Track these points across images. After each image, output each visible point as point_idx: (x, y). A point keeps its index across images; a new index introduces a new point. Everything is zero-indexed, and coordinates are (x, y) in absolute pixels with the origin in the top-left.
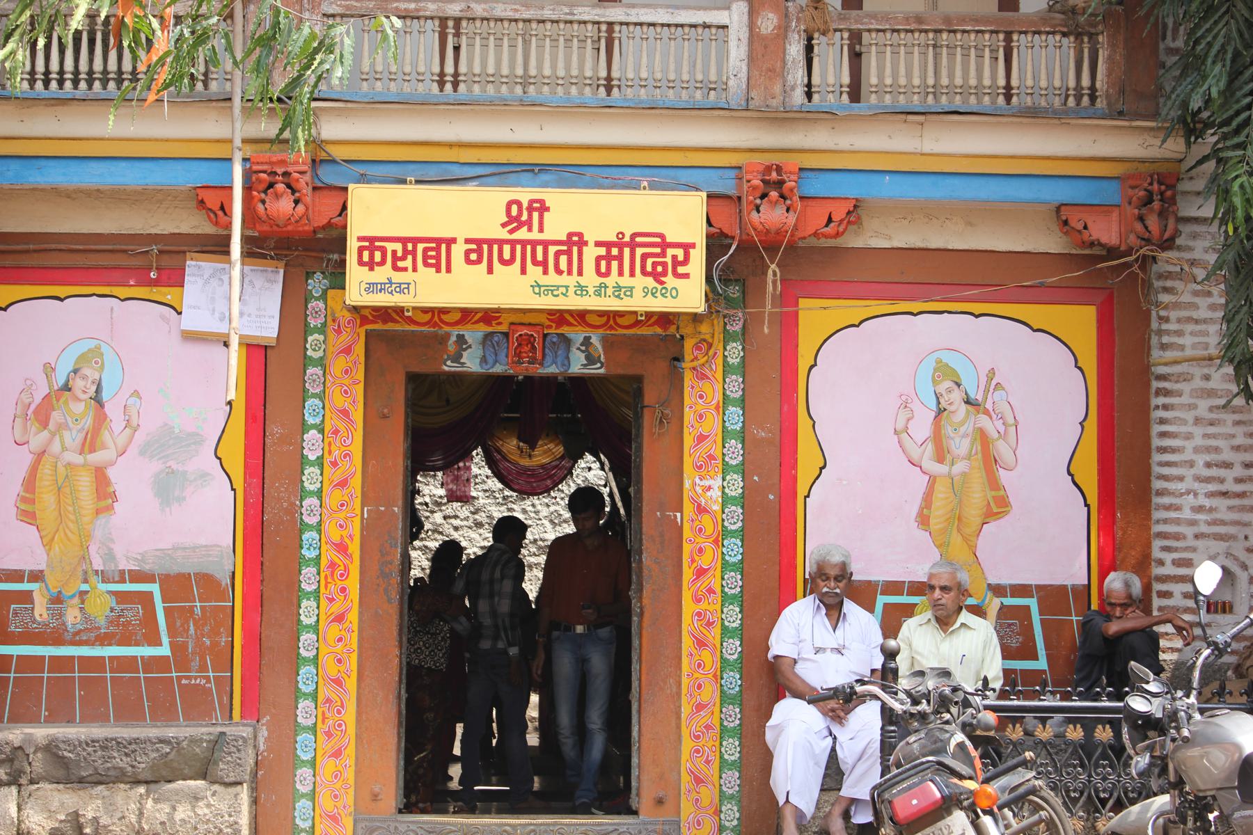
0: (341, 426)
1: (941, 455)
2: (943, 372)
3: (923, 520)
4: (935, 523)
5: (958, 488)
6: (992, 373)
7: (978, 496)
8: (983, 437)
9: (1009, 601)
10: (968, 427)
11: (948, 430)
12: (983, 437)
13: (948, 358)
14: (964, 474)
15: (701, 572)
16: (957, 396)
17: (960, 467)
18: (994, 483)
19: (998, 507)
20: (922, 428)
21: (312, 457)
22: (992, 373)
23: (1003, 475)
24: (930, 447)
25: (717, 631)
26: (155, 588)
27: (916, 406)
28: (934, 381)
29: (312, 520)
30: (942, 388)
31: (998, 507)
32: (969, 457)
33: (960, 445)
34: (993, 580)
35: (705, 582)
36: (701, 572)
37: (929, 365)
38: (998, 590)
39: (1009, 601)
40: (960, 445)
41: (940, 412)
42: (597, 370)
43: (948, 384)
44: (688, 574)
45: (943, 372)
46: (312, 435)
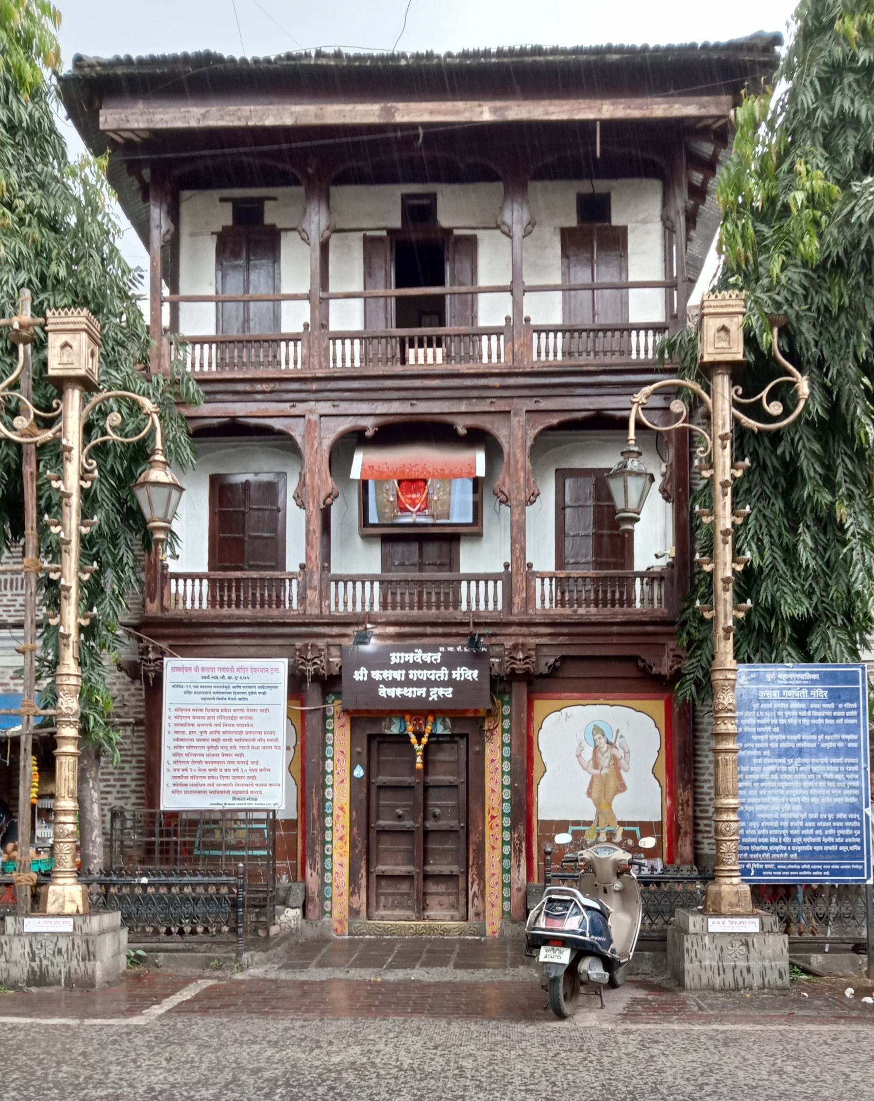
0: (342, 758)
1: (596, 765)
2: (597, 730)
3: (589, 794)
4: (595, 794)
5: (604, 781)
6: (618, 731)
7: (612, 784)
8: (615, 759)
9: (627, 828)
10: (608, 754)
11: (599, 755)
12: (615, 759)
13: (598, 724)
14: (606, 775)
15: (493, 817)
16: (603, 740)
17: (604, 771)
18: (619, 778)
19: (622, 787)
20: (588, 754)
21: (329, 770)
22: (618, 731)
23: (624, 774)
24: (591, 763)
25: (499, 843)
26: (264, 826)
27: (585, 745)
28: (593, 735)
29: (329, 797)
30: (597, 737)
31: (622, 787)
32: (608, 766)
33: (605, 761)
34: (619, 819)
35: (495, 822)
36: (493, 817)
37: (591, 727)
38: (621, 824)
39: (627, 828)
40: (605, 761)
41: (596, 747)
42: (447, 732)
43: (599, 735)
44: (488, 818)
45: (597, 730)
46: (329, 762)
